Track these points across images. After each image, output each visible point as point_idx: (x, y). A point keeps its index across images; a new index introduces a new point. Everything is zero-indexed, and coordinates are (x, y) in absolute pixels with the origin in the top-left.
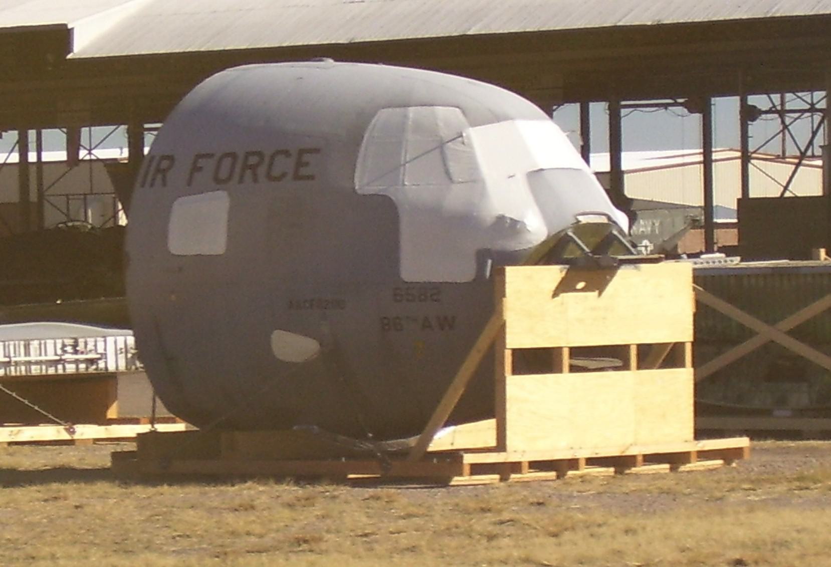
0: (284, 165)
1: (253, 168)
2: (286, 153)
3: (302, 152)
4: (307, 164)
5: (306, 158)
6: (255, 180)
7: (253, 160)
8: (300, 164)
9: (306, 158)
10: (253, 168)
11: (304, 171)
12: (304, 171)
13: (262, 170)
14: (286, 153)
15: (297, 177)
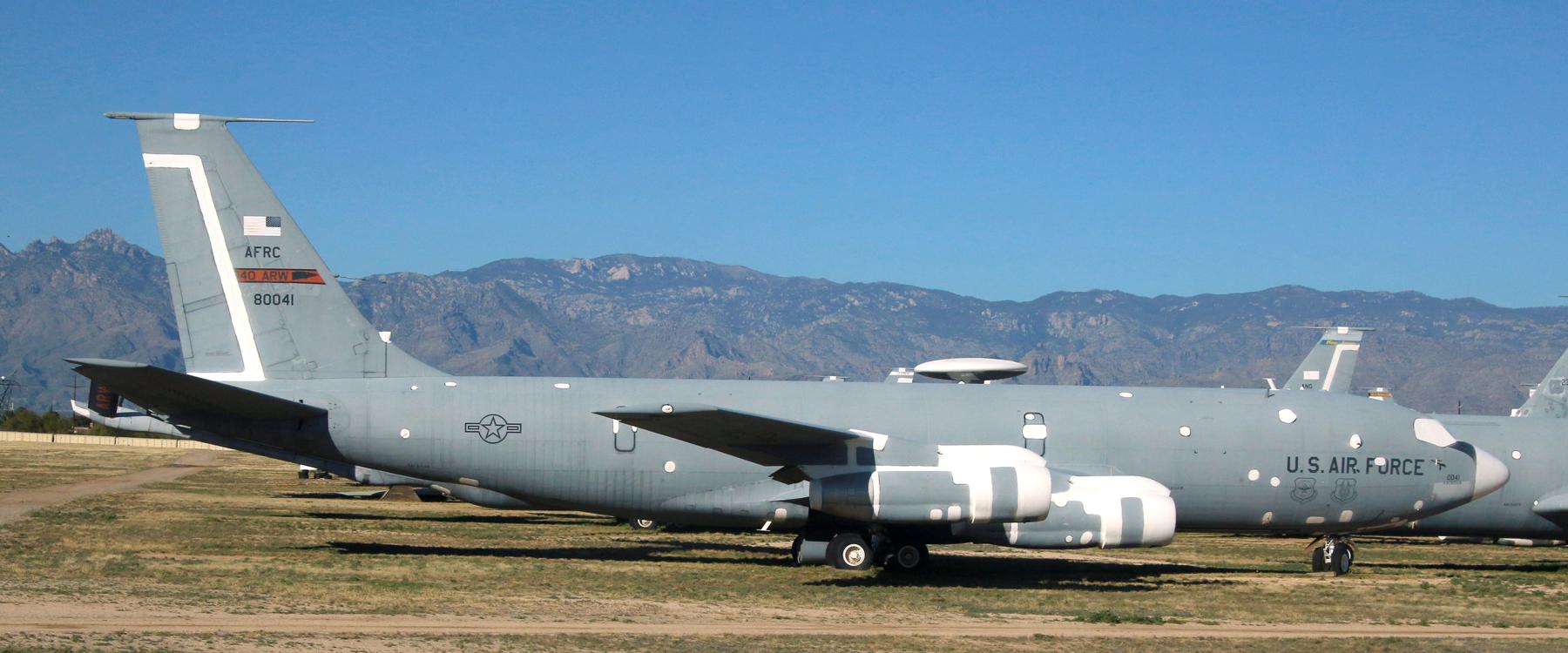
0: (1410, 467)
1: (1397, 467)
2: (1411, 462)
3: (1417, 461)
4: (1419, 467)
5: (1419, 464)
6: (1398, 473)
7: (1396, 463)
8: (1417, 467)
9: (1419, 464)
10: (1397, 467)
11: (1418, 471)
12: (1418, 471)
13: (1401, 469)
14: (1411, 462)
15: (1416, 474)
